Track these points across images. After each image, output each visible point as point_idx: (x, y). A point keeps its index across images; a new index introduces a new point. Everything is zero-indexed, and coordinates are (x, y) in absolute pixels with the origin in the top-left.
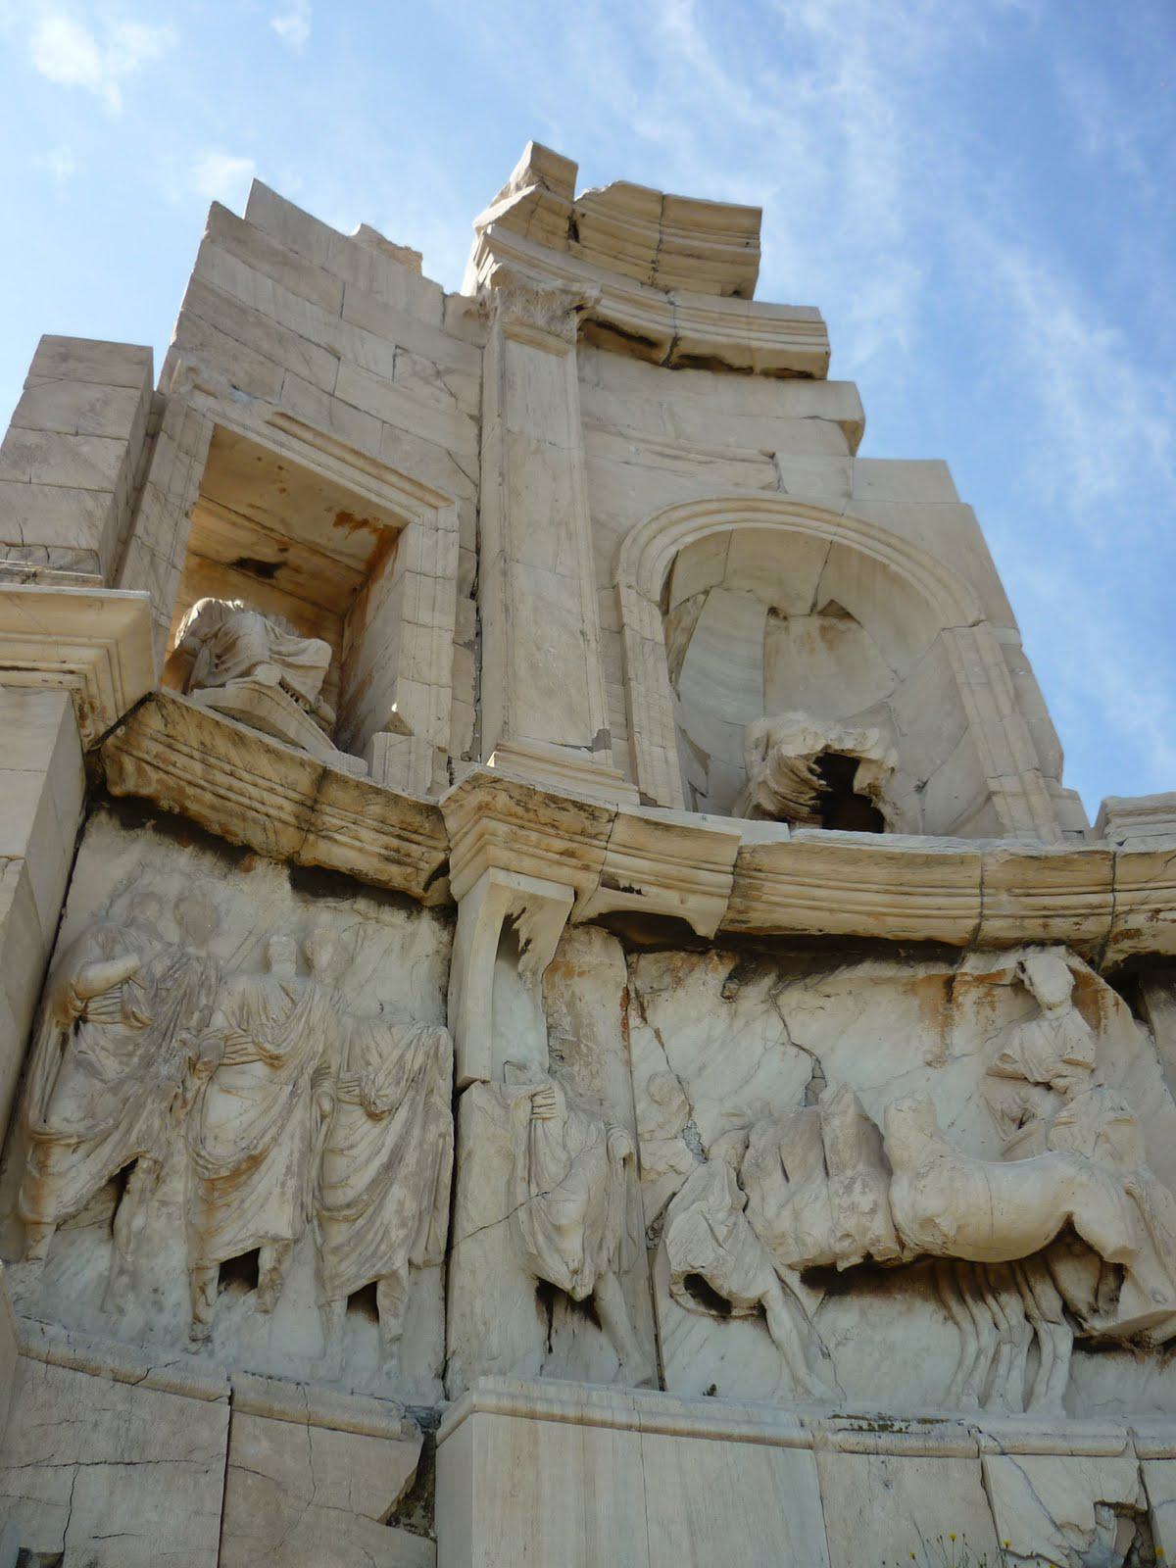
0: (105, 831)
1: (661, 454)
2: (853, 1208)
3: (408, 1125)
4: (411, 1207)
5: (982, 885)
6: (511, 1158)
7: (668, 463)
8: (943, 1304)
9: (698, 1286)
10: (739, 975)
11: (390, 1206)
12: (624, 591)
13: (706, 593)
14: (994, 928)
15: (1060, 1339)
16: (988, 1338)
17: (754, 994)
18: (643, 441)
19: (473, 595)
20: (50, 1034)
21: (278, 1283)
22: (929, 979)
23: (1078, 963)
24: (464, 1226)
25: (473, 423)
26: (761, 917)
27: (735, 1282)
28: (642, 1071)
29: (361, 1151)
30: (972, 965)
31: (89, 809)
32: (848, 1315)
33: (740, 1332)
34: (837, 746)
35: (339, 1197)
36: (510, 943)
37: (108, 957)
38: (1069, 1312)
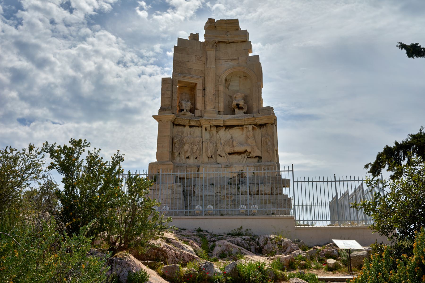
0: (175, 127)
1: (226, 61)
2: (230, 149)
3: (198, 146)
4: (199, 152)
5: (244, 121)
6: (205, 148)
8: (238, 155)
9: (219, 155)
10: (226, 129)
11: (197, 153)
12: (219, 85)
13: (231, 77)
14: (246, 124)
15: (246, 157)
16: (241, 158)
18: (224, 59)
19: (204, 90)
20: (174, 145)
21: (190, 158)
22: (241, 128)
23: (254, 126)
24: (203, 152)
25: (204, 65)
26: (226, 125)
28: (217, 138)
29: (195, 148)
30: (244, 127)
31: (173, 125)
32: (231, 156)
33: (223, 158)
34: (237, 103)
35: (194, 152)
36: (206, 130)
37: (176, 139)
38: (247, 155)
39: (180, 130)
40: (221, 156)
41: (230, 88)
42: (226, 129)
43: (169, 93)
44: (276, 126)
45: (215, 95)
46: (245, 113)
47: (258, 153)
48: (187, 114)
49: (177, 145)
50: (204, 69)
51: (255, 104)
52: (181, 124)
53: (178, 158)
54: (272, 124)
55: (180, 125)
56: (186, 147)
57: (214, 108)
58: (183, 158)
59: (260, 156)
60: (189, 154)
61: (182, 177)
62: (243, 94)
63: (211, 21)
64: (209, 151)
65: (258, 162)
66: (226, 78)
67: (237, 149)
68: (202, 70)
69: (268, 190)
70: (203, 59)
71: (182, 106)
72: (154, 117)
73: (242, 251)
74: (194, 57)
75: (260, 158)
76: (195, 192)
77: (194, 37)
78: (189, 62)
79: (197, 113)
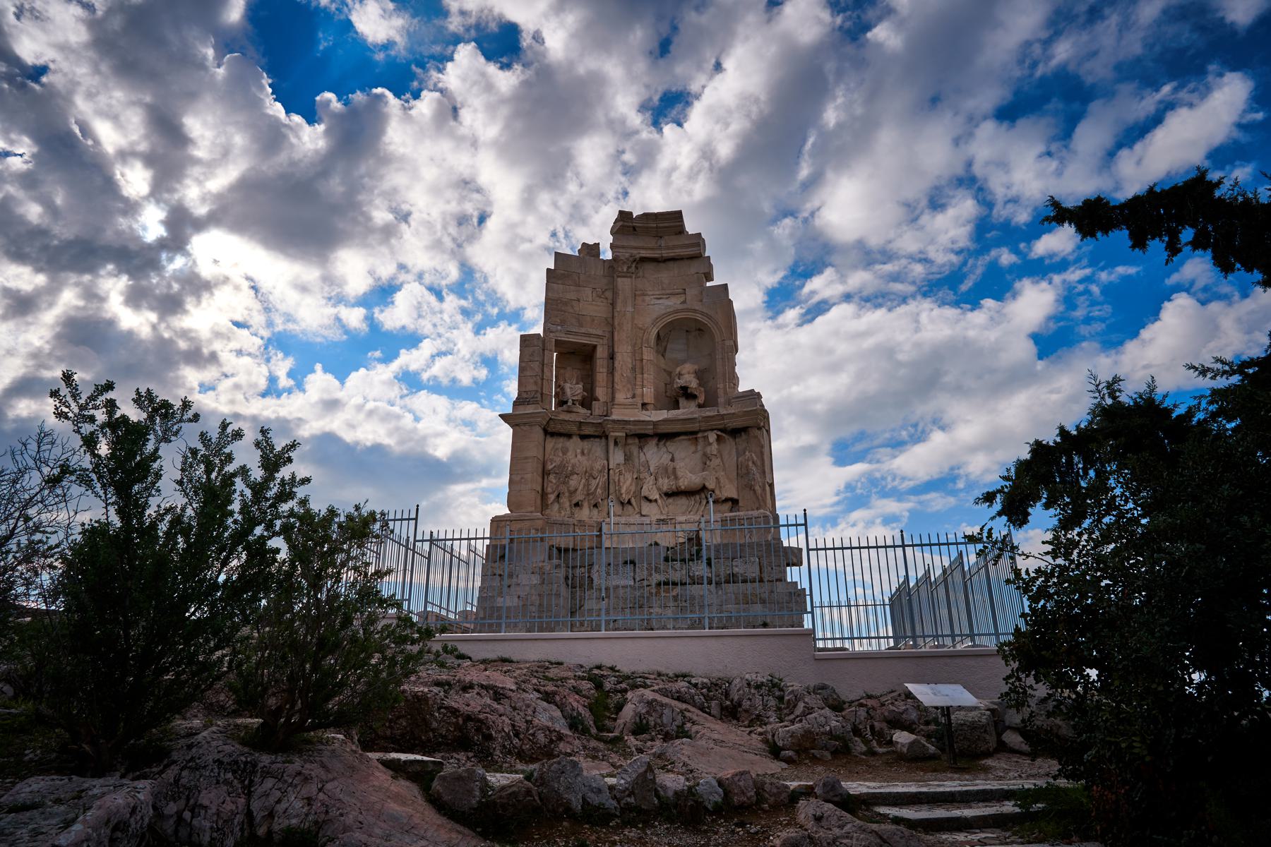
0: (549, 439)
7: (661, 301)
9: (647, 499)
10: (659, 441)
17: (662, 443)
23: (719, 433)
26: (659, 431)
27: (651, 498)
32: (670, 500)
33: (654, 504)
36: (616, 443)
39: (560, 446)
40: (650, 501)
41: (668, 354)
42: (659, 441)
43: (536, 366)
44: (768, 432)
45: (634, 369)
46: (700, 406)
47: (730, 491)
48: (575, 410)
49: (552, 477)
50: (610, 315)
51: (721, 386)
52: (562, 431)
53: (556, 507)
54: (759, 429)
55: (560, 435)
56: (573, 482)
57: (634, 396)
58: (567, 504)
59: (735, 496)
60: (579, 497)
61: (563, 546)
62: (696, 367)
63: (624, 216)
64: (623, 491)
65: (731, 511)
66: (658, 333)
67: (683, 484)
68: (606, 319)
69: (753, 571)
70: (609, 294)
71: (564, 393)
72: (503, 416)
73: (687, 714)
74: (588, 291)
75: (734, 502)
76: (592, 580)
77: (591, 250)
78: (579, 300)
79: (598, 408)
